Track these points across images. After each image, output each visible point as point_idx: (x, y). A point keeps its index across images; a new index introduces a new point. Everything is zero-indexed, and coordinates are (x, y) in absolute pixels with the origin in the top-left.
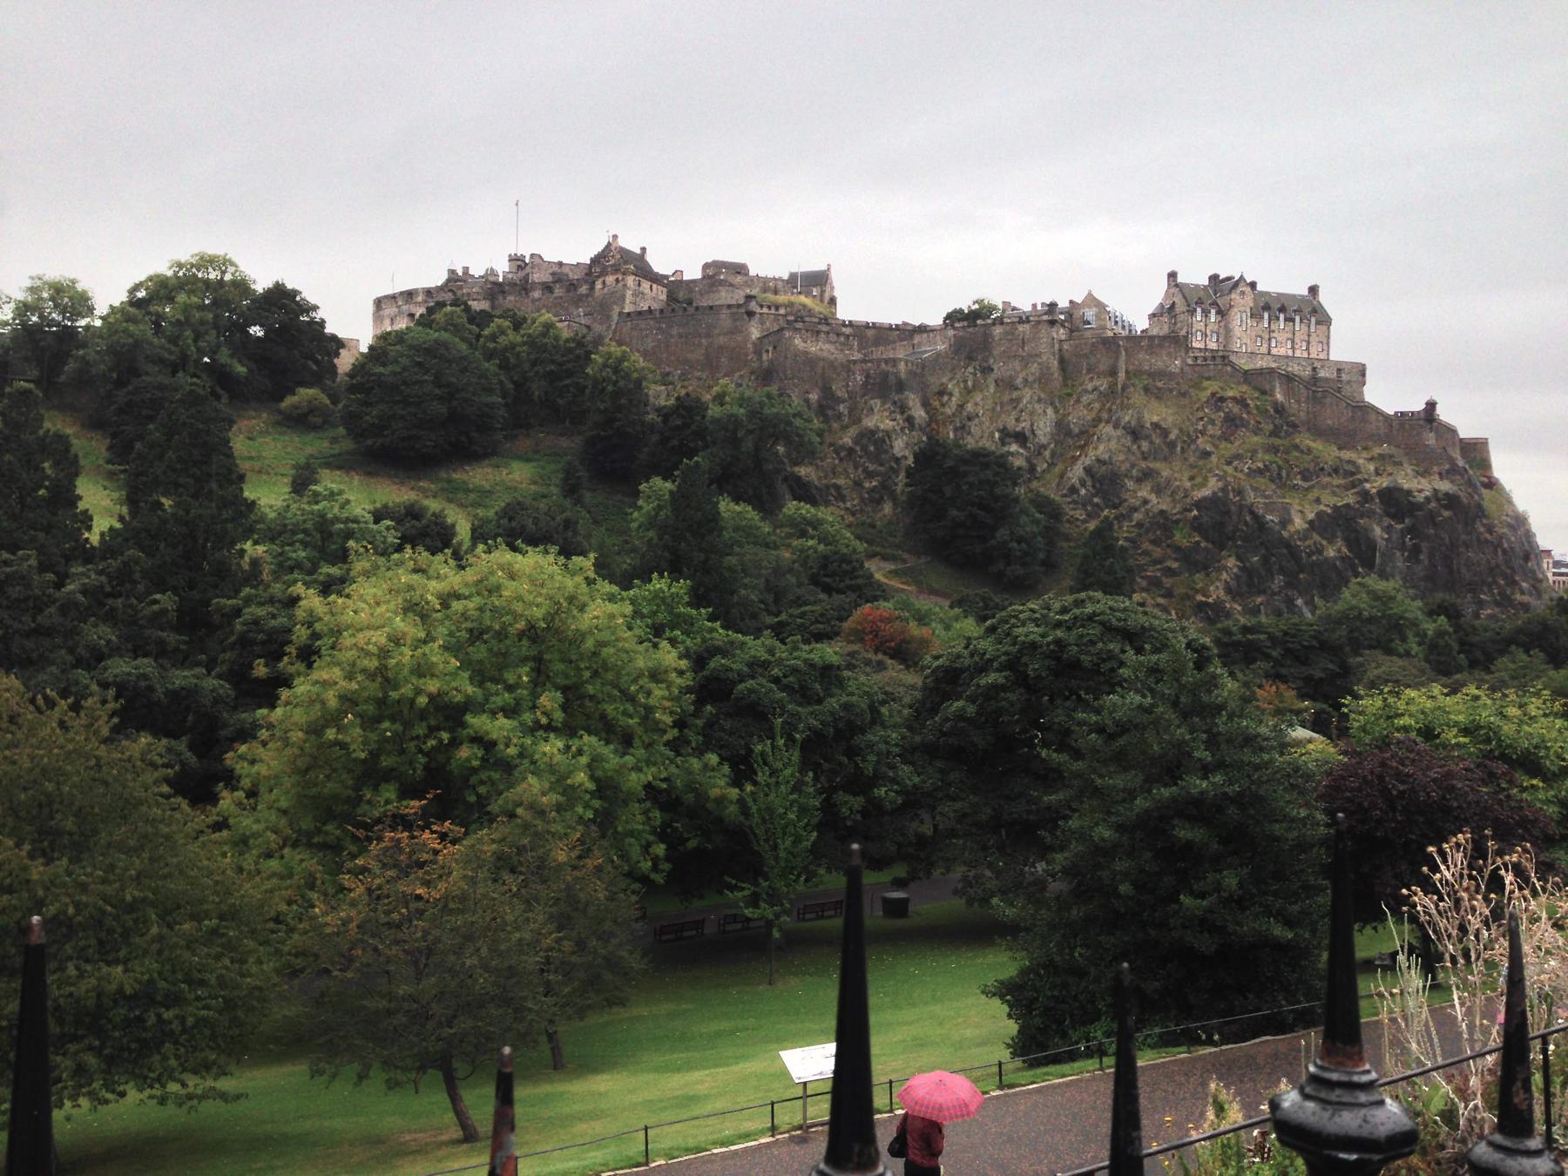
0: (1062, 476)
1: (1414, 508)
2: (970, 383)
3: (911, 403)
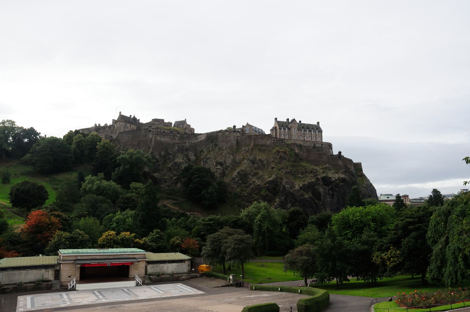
3: (190, 155)
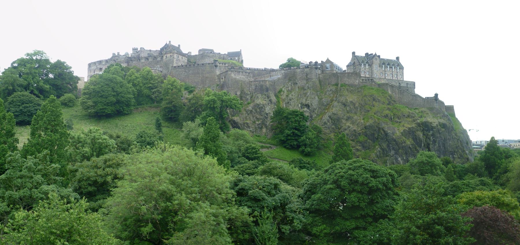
0: (321, 119)
1: (432, 128)
2: (290, 88)
3: (271, 95)
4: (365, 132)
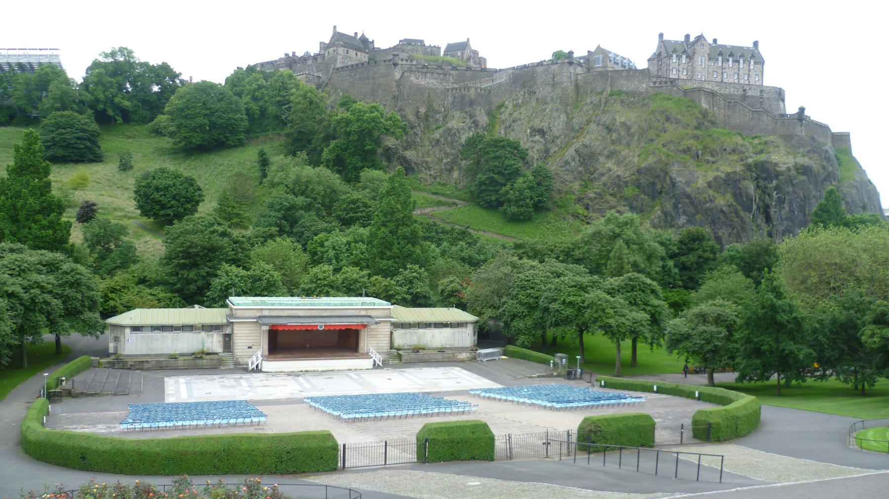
1: (777, 175)
3: (478, 112)
4: (638, 180)
